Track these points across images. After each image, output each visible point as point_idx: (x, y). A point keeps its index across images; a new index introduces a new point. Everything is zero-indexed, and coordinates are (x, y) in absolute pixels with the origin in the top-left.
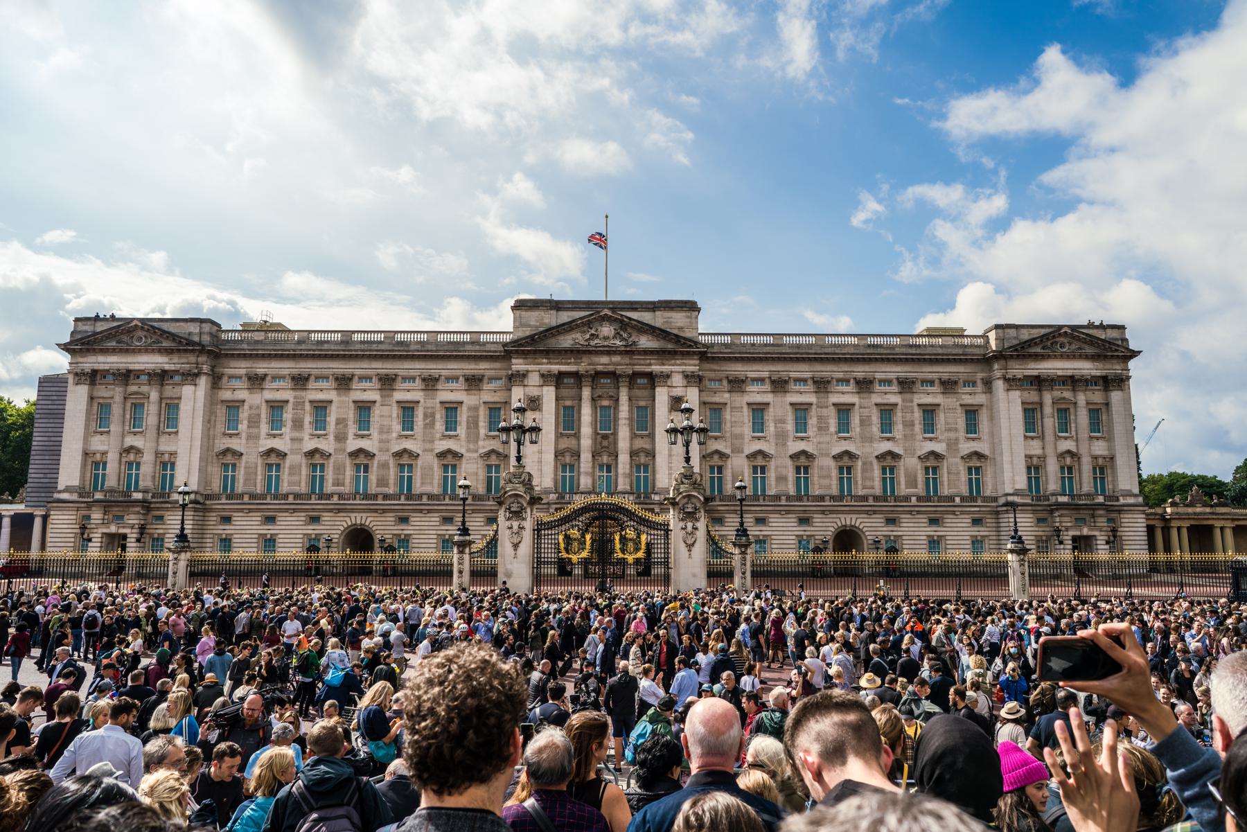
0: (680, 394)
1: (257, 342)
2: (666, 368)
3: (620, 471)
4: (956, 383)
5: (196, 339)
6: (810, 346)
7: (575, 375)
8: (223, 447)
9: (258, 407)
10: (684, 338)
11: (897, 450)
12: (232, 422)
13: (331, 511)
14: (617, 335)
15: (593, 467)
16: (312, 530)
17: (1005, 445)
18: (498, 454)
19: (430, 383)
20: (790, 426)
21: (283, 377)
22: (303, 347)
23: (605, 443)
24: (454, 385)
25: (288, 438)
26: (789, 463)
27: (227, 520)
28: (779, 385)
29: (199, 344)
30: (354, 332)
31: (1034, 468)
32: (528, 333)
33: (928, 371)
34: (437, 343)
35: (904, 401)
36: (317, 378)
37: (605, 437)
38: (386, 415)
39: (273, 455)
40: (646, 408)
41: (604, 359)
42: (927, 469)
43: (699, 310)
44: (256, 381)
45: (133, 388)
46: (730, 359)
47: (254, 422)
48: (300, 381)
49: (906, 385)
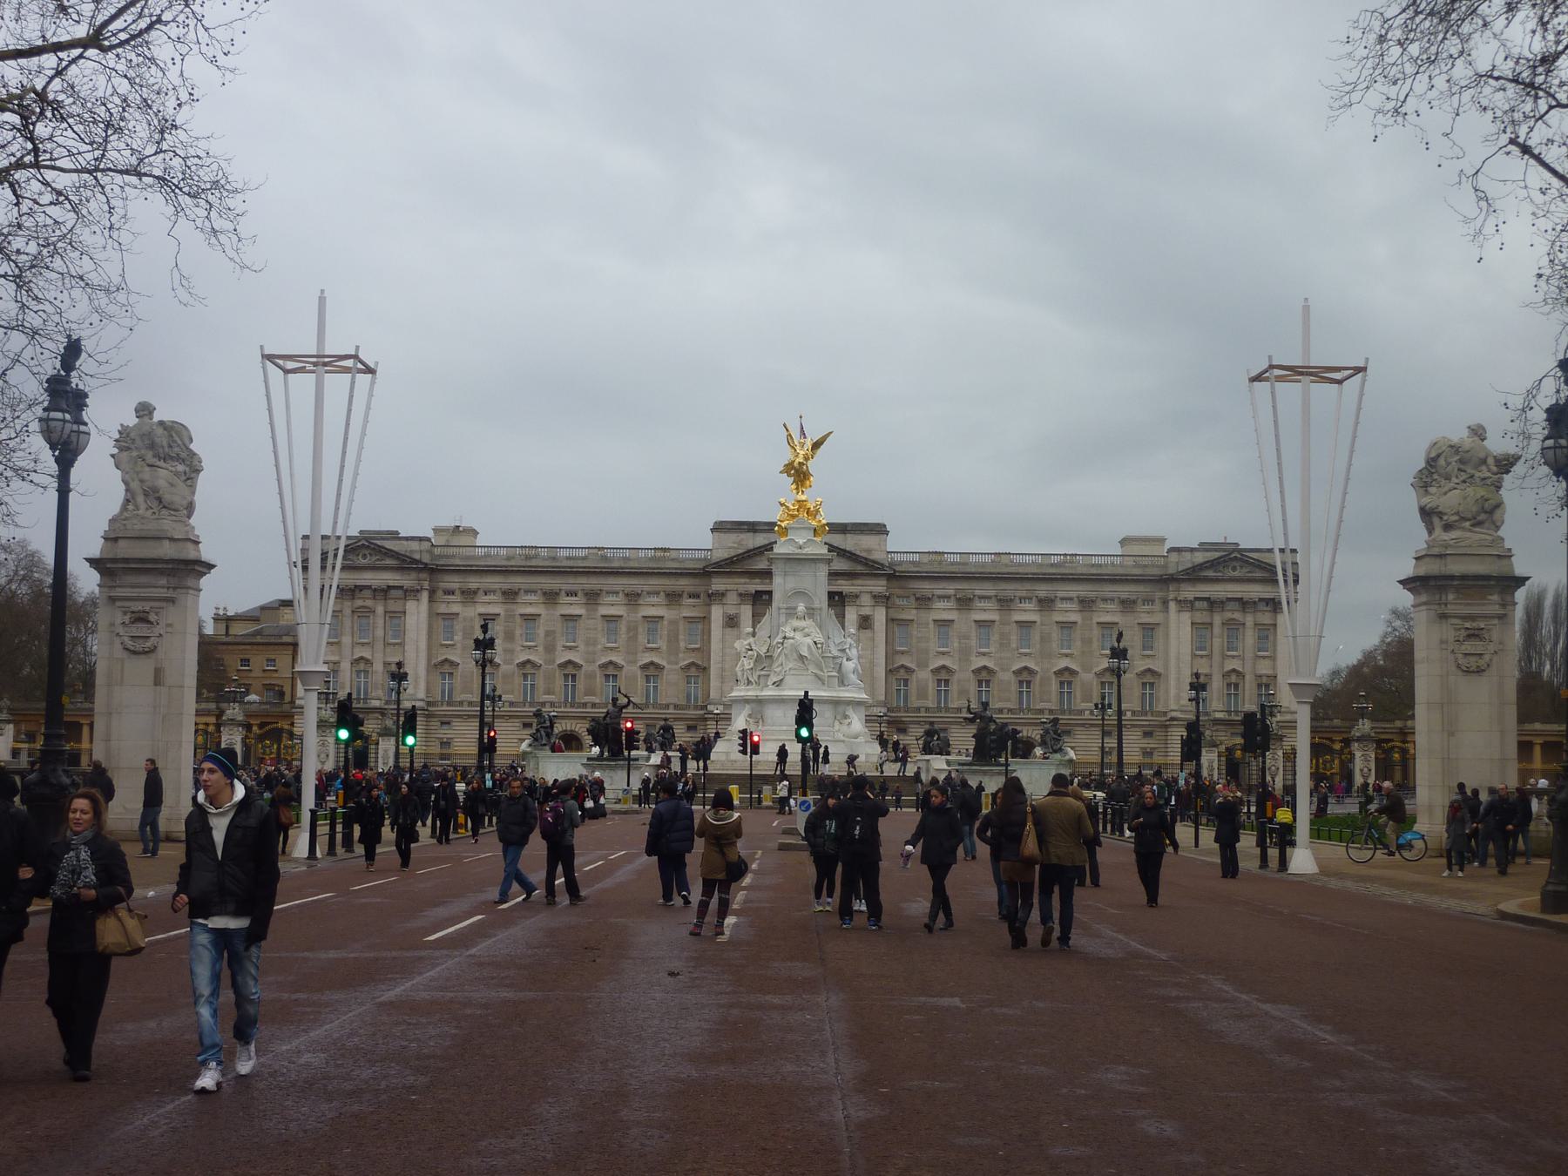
1: (468, 558)
4: (1134, 602)
5: (417, 557)
9: (472, 620)
11: (1073, 667)
12: (450, 633)
17: (1173, 663)
18: (697, 666)
19: (633, 598)
20: (973, 643)
21: (494, 592)
24: (654, 600)
28: (965, 603)
29: (419, 562)
31: (1198, 686)
32: (726, 556)
33: (1108, 590)
34: (638, 559)
36: (527, 592)
43: (887, 533)
44: (469, 595)
45: (359, 603)
48: (510, 595)
49: (1086, 604)
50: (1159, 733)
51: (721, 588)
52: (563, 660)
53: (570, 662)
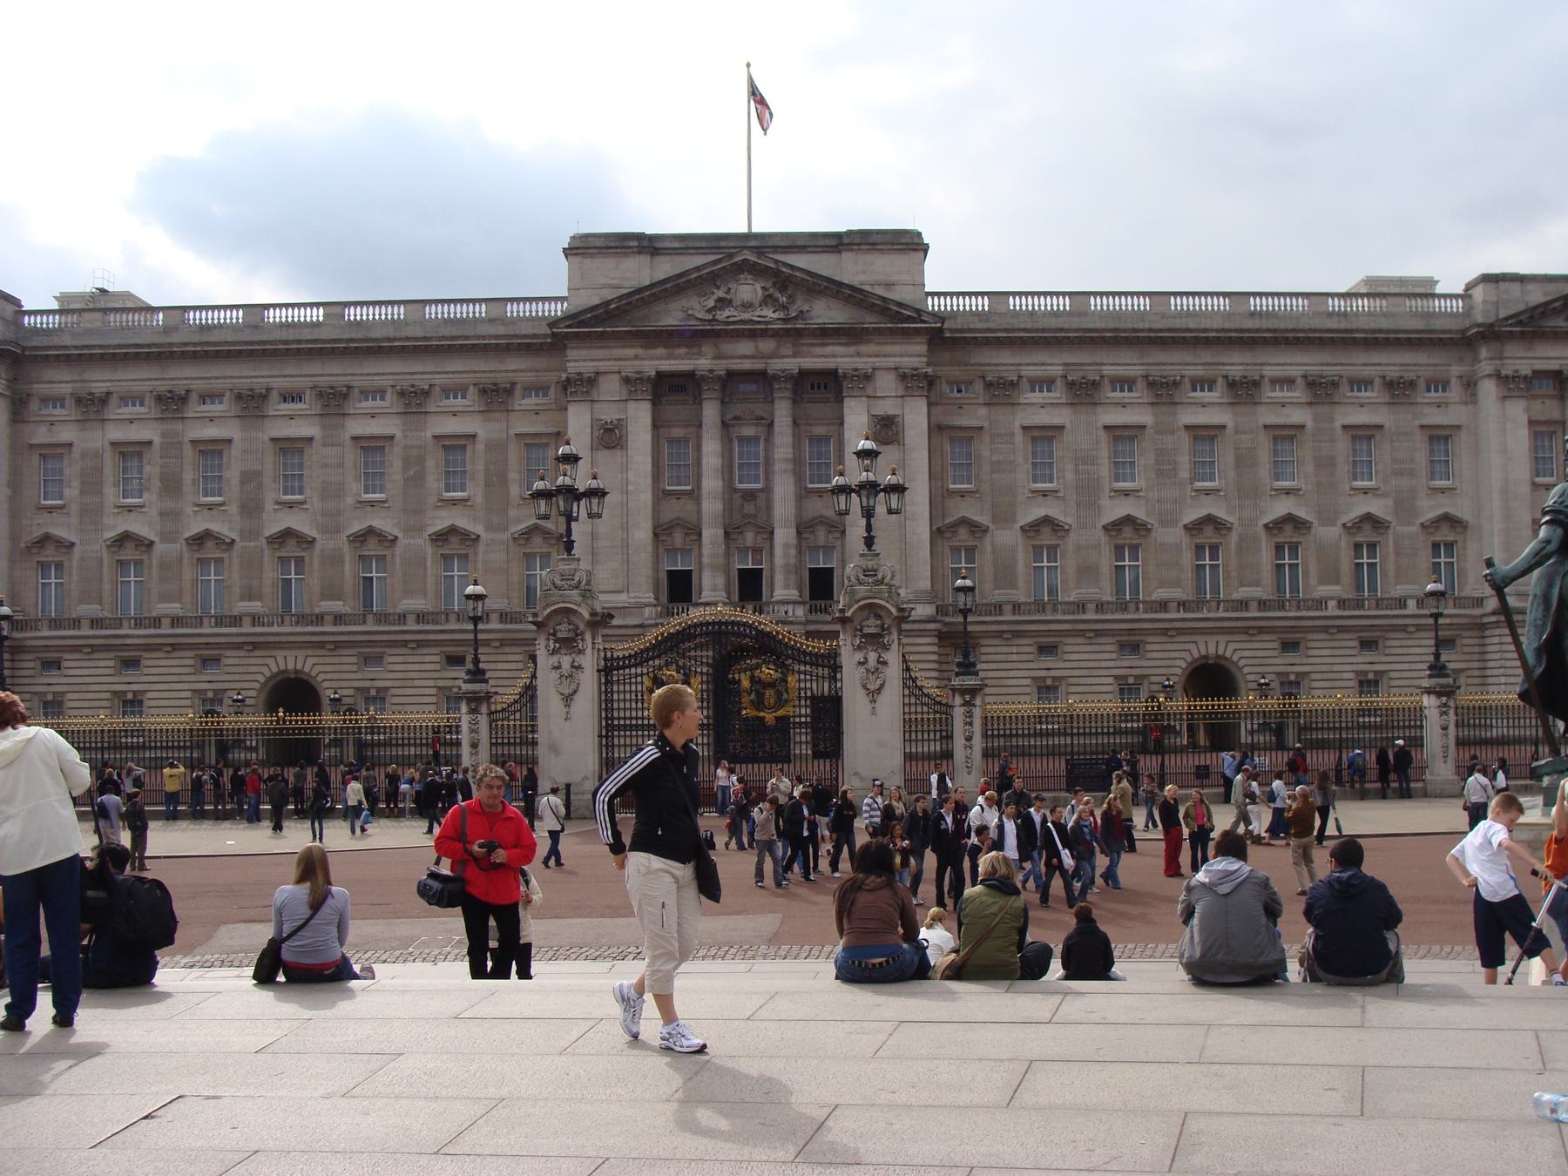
0: (890, 412)
2: (864, 363)
3: (779, 561)
4: (1412, 384)
6: (1142, 315)
7: (691, 375)
8: (38, 533)
9: (98, 455)
10: (899, 304)
11: (1302, 513)
13: (239, 646)
14: (768, 300)
15: (728, 554)
16: (208, 680)
18: (546, 533)
19: (414, 400)
20: (1104, 470)
22: (175, 338)
23: (749, 508)
24: (458, 403)
25: (153, 512)
26: (1104, 538)
27: (53, 665)
28: (1083, 392)
30: (267, 307)
32: (596, 301)
34: (423, 322)
35: (1316, 419)
36: (204, 398)
37: (749, 495)
38: (333, 460)
39: (130, 546)
40: (827, 439)
41: (745, 347)
42: (1358, 547)
43: (924, 249)
44: (93, 406)
46: (987, 342)
47: (92, 484)
48: (172, 403)
49: (1321, 390)
50: (1468, 641)
51: (587, 368)
52: (274, 528)
53: (288, 534)
